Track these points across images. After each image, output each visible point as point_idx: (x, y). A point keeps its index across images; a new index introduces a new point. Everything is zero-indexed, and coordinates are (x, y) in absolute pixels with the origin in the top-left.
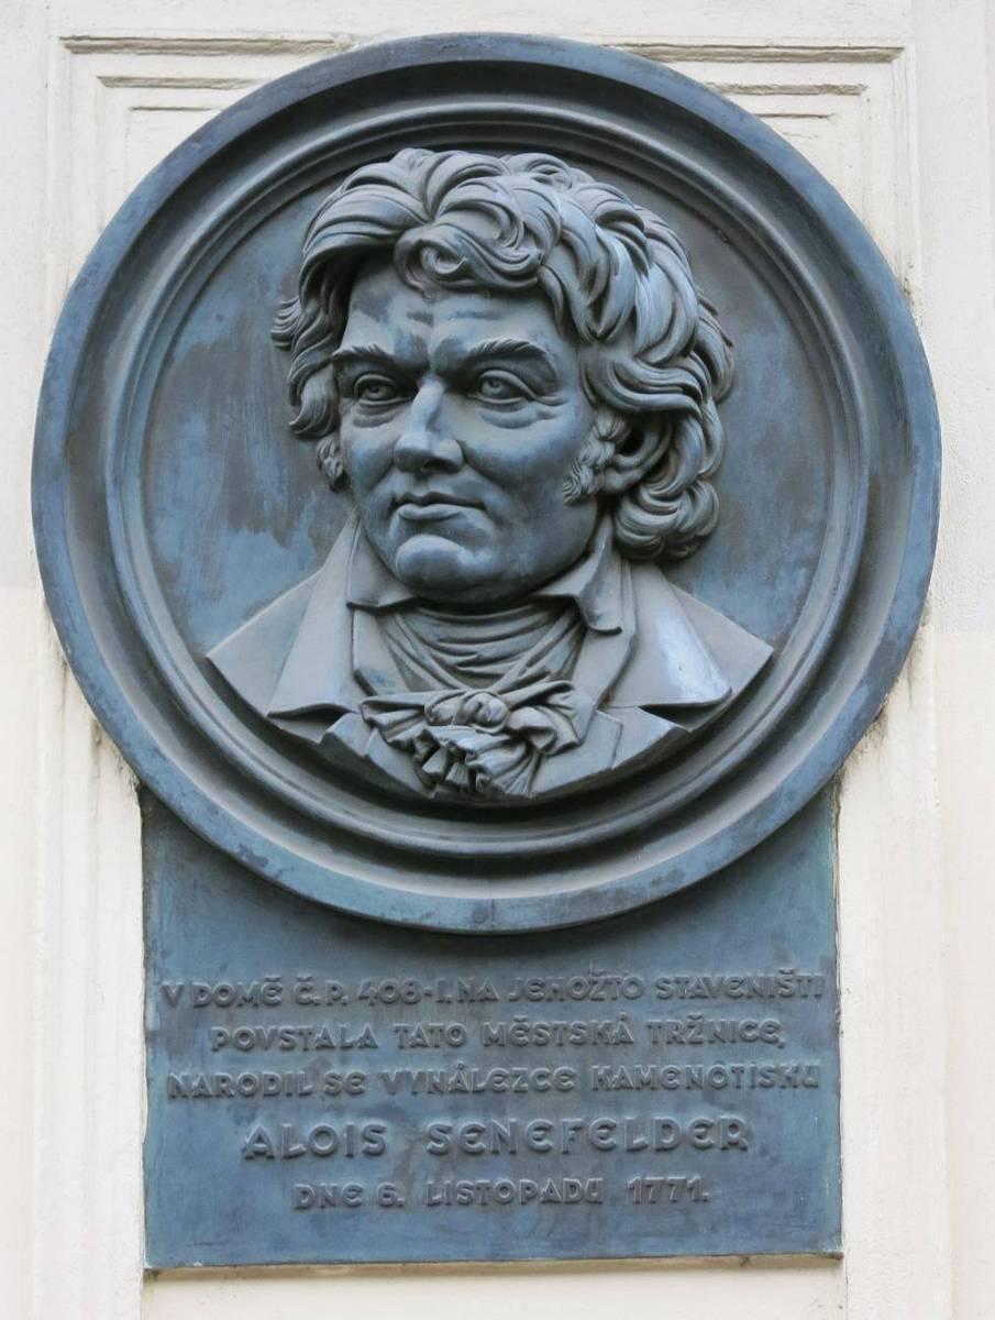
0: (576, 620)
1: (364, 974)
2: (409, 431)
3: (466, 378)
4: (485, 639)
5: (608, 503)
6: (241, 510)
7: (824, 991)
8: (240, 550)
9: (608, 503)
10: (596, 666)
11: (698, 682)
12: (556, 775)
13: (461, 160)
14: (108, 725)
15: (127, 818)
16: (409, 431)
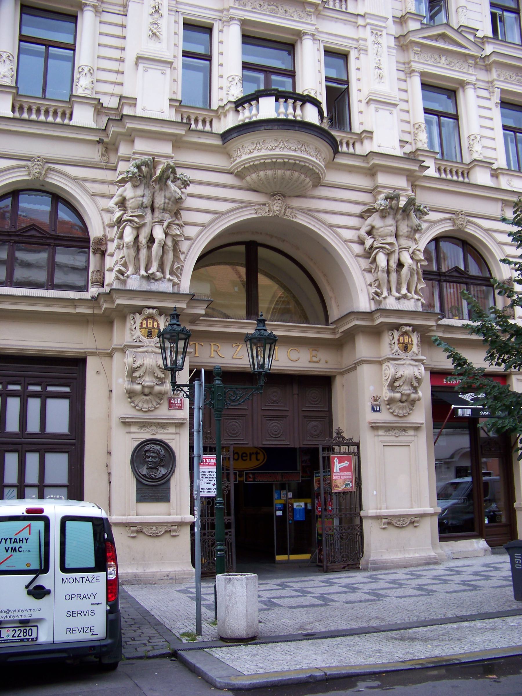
0: (158, 469)
1: (147, 487)
2: (150, 460)
3: (152, 457)
4: (153, 470)
5: (159, 463)
6: (141, 463)
7: (170, 488)
8: (141, 466)
9: (159, 463)
10: (159, 472)
11: (164, 473)
12: (157, 477)
13: (153, 445)
14: (134, 474)
15: (135, 479)
16: (150, 460)
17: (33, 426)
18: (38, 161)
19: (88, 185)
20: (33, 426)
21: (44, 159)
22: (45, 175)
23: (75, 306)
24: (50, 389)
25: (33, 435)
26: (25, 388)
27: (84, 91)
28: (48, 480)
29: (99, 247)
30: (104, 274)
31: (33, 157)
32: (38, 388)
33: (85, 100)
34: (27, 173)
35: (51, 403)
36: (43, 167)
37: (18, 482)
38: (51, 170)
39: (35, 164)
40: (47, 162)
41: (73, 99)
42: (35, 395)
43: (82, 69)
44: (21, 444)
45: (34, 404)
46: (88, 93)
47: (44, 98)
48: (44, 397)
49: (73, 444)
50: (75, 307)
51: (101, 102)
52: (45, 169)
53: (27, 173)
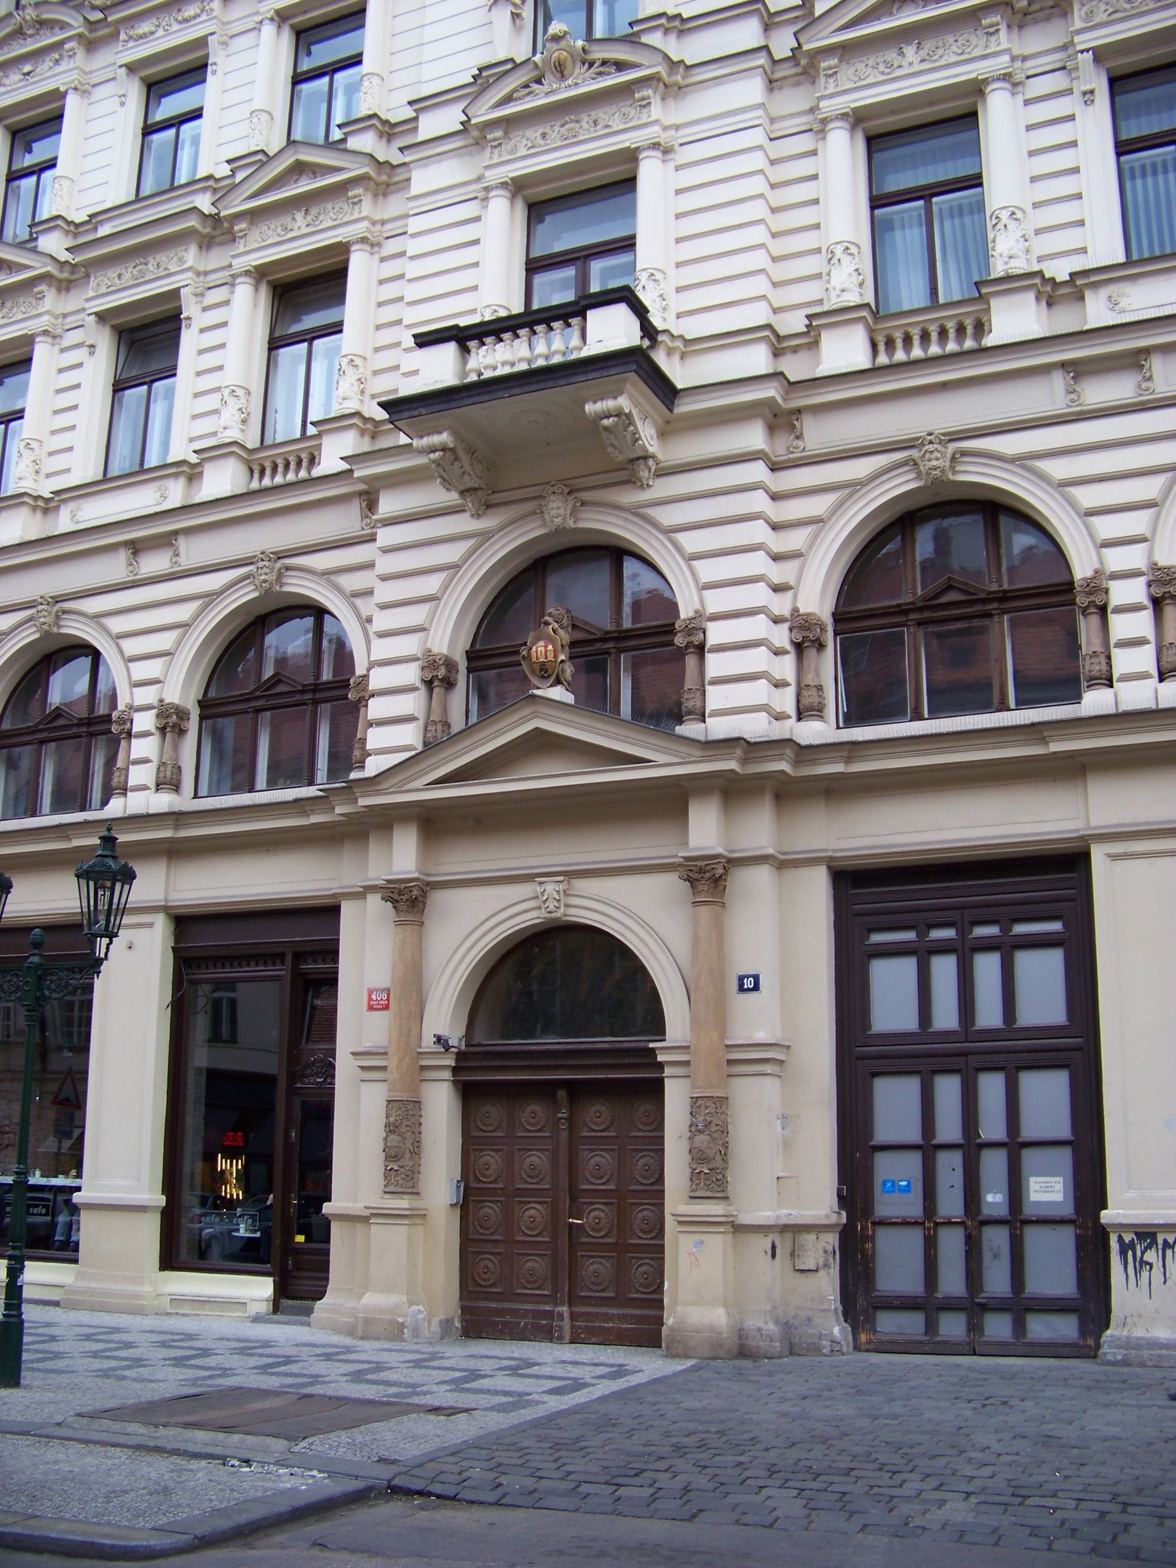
17: (989, 1015)
18: (931, 442)
19: (1045, 466)
20: (989, 1015)
21: (944, 434)
22: (952, 468)
23: (1044, 738)
24: (1020, 929)
25: (990, 1034)
26: (963, 933)
27: (1006, 263)
28: (1028, 1131)
29: (1092, 598)
30: (1109, 657)
31: (918, 439)
32: (992, 930)
33: (1012, 282)
34: (913, 475)
35: (1025, 961)
36: (943, 455)
37: (964, 1137)
38: (964, 453)
39: (926, 451)
40: (950, 441)
41: (984, 291)
42: (987, 946)
43: (997, 217)
44: (963, 1054)
45: (987, 966)
46: (1020, 266)
47: (935, 305)
48: (1007, 948)
49: (1078, 1049)
50: (1044, 741)
51: (1047, 276)
52: (949, 456)
53: (913, 475)
